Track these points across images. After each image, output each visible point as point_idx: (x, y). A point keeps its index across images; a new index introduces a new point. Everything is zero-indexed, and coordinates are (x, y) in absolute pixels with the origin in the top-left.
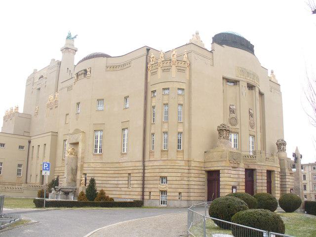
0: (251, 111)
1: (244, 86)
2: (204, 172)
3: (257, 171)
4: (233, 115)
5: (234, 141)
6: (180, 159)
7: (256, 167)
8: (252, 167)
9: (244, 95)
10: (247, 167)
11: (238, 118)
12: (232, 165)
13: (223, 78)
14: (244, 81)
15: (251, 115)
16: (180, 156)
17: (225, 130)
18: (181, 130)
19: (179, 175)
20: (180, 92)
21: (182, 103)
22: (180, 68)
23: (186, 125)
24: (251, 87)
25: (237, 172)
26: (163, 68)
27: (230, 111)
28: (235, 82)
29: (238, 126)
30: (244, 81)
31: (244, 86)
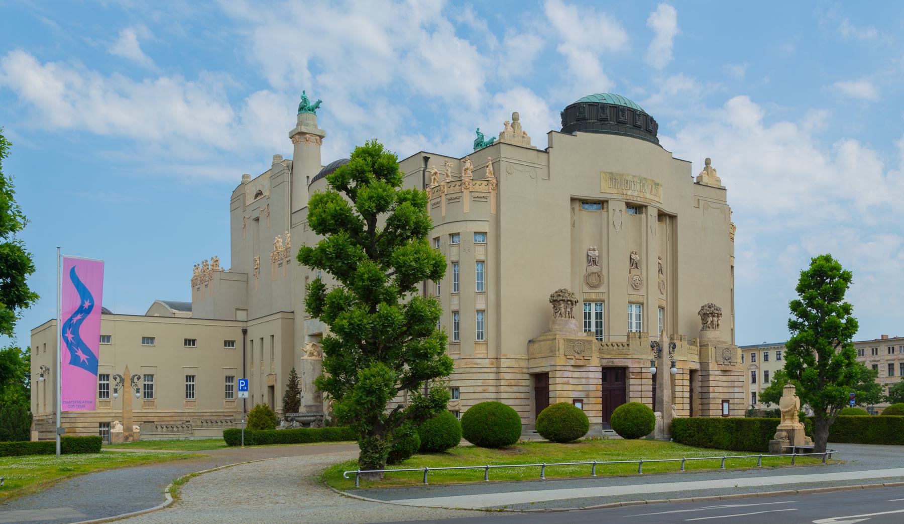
0: (633, 256)
1: (617, 210)
2: (527, 376)
3: (631, 370)
4: (594, 269)
5: (597, 318)
6: (481, 356)
7: (629, 364)
8: (619, 363)
9: (618, 227)
10: (605, 363)
11: (604, 273)
12: (573, 362)
13: (573, 200)
14: (619, 200)
15: (634, 264)
16: (481, 351)
17: (563, 301)
18: (481, 306)
19: (479, 383)
20: (479, 238)
21: (482, 258)
22: (477, 194)
23: (492, 297)
24: (637, 208)
25: (584, 375)
26: (449, 197)
27: (589, 261)
28: (601, 203)
29: (603, 289)
30: (619, 200)
31: (617, 210)
